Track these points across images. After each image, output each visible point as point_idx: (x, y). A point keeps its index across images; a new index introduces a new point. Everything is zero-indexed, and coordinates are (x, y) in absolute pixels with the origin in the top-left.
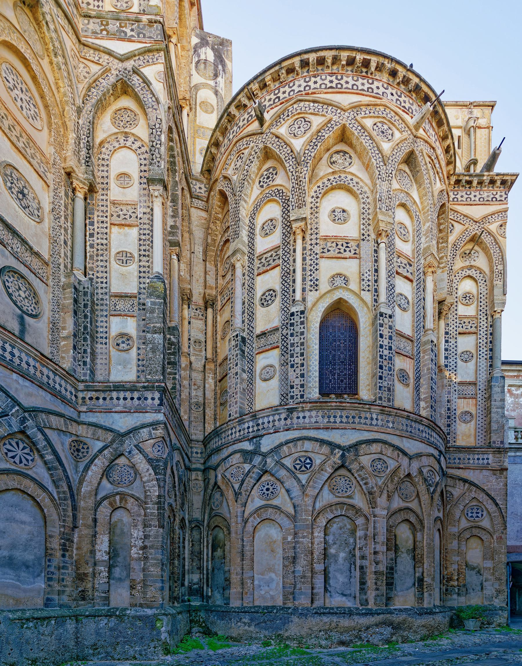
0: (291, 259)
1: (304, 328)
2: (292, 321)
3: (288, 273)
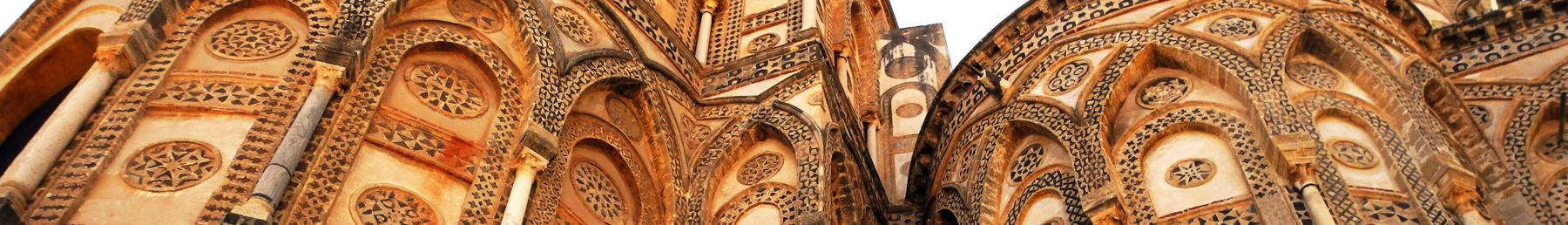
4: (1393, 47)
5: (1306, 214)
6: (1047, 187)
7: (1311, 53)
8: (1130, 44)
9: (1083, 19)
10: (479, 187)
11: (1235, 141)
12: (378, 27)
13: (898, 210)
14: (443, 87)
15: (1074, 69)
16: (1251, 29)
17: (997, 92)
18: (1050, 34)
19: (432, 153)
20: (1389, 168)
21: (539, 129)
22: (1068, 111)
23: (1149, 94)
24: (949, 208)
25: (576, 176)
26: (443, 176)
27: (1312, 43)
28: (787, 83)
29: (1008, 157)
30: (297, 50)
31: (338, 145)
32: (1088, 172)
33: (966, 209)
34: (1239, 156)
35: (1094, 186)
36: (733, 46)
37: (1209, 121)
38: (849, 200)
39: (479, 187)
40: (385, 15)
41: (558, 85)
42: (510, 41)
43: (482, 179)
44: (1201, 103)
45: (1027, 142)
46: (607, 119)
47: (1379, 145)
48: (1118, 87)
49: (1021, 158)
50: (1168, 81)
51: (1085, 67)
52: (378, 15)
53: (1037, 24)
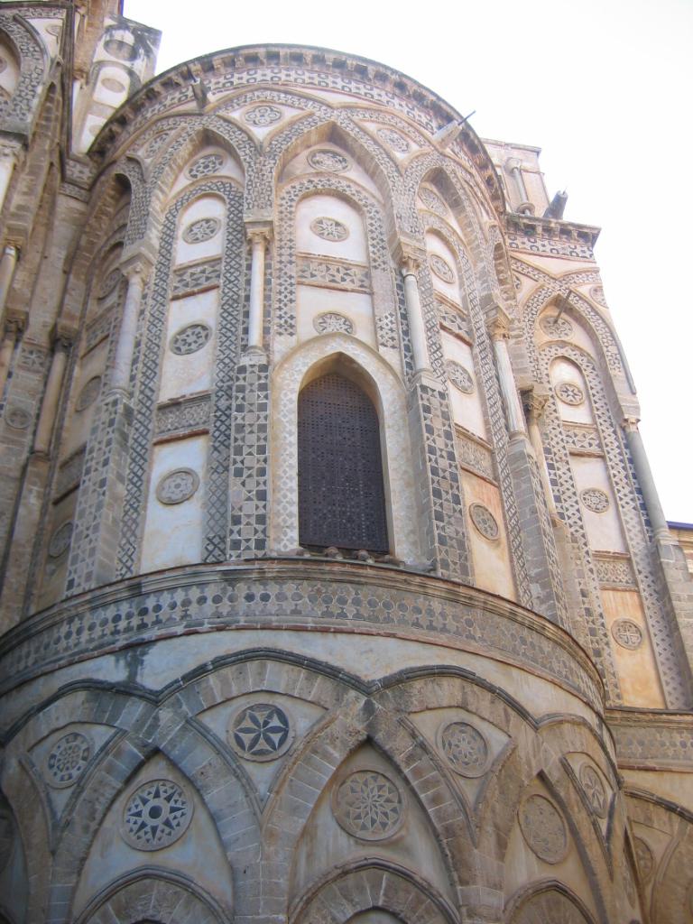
0: (242, 279)
1: (266, 397)
2: (241, 382)
3: (235, 301)
5: (403, 295)
6: (217, 192)
8: (318, 114)
9: (288, 78)
11: (369, 221)
15: (269, 112)
16: (404, 148)
17: (202, 101)
18: (259, 77)
20: (460, 288)
22: (256, 141)
23: (318, 158)
24: (127, 174)
27: (438, 178)
29: (192, 155)
32: (256, 194)
33: (143, 181)
34: (368, 233)
35: (258, 206)
37: (356, 198)
44: (355, 183)
45: (210, 150)
47: (459, 270)
48: (298, 141)
49: (202, 161)
50: (335, 154)
51: (278, 115)
53: (251, 65)
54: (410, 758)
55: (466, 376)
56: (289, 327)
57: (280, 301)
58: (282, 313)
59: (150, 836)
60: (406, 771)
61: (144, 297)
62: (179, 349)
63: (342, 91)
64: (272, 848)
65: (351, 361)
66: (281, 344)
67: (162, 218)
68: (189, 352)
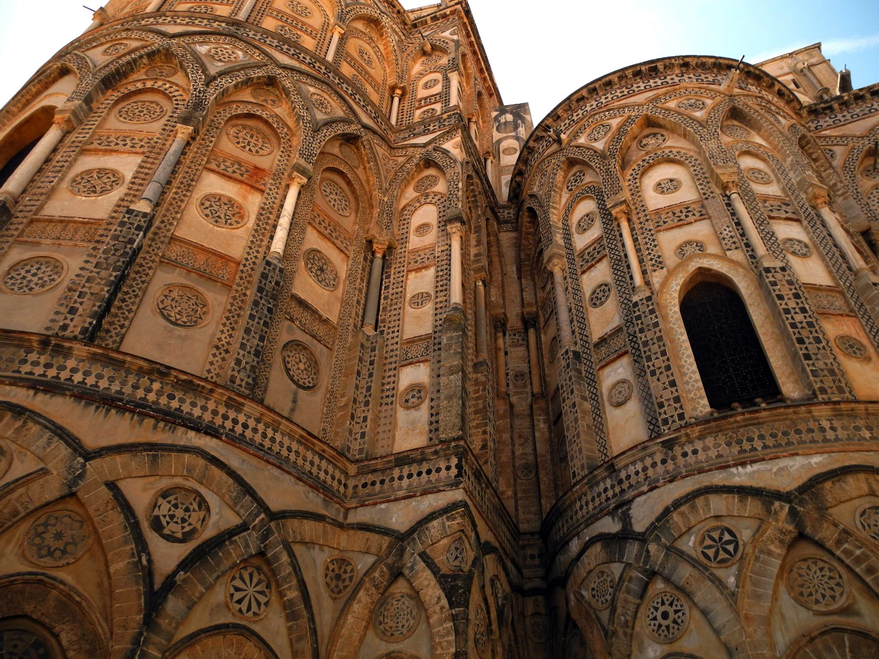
0: (619, 245)
1: (656, 317)
2: (638, 313)
3: (620, 261)
4: (781, 116)
7: (735, 119)
8: (633, 114)
10: (269, 194)
11: (692, 169)
12: (212, 105)
13: (504, 207)
14: (249, 138)
16: (701, 106)
17: (559, 141)
18: (588, 108)
19: (242, 175)
21: (302, 162)
23: (644, 142)
25: (323, 188)
26: (248, 188)
27: (735, 114)
28: (441, 136)
29: (565, 177)
30: (166, 118)
31: (190, 171)
33: (541, 207)
34: (694, 177)
36: (411, 115)
37: (678, 157)
38: (476, 201)
39: (269, 194)
40: (216, 98)
41: (313, 137)
42: (286, 113)
43: (270, 189)
44: (673, 147)
45: (575, 169)
46: (340, 156)
47: (773, 171)
50: (655, 135)
52: (212, 98)
53: (581, 103)
54: (839, 543)
55: (802, 245)
56: (659, 264)
57: (648, 249)
58: (651, 256)
59: (666, 632)
60: (838, 553)
61: (565, 278)
62: (595, 304)
63: (646, 90)
64: (751, 629)
65: (709, 270)
66: (657, 278)
67: (560, 225)
68: (602, 304)
